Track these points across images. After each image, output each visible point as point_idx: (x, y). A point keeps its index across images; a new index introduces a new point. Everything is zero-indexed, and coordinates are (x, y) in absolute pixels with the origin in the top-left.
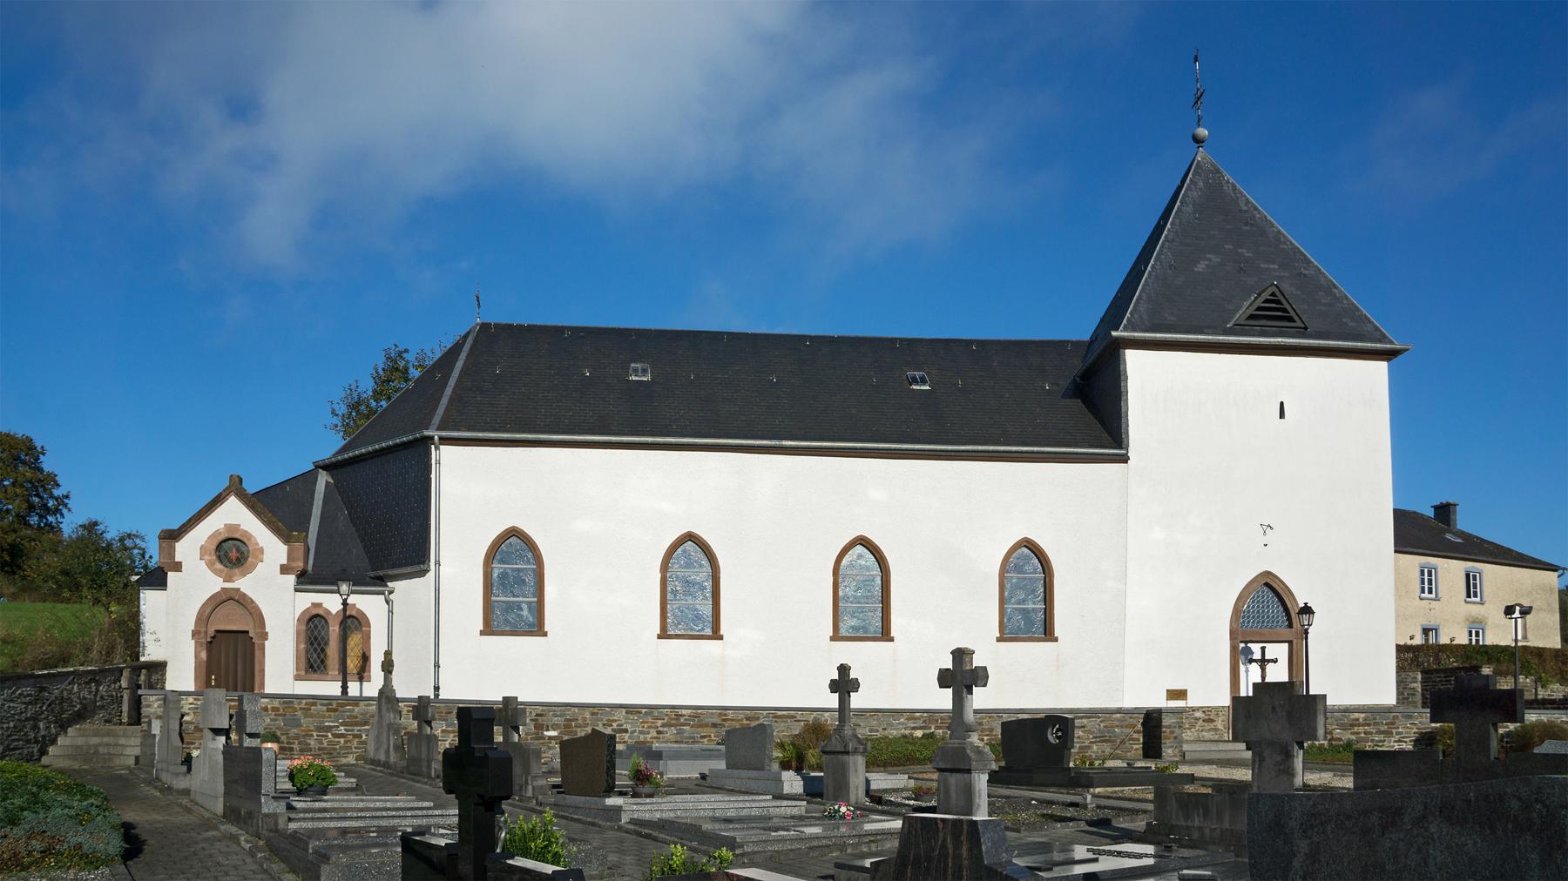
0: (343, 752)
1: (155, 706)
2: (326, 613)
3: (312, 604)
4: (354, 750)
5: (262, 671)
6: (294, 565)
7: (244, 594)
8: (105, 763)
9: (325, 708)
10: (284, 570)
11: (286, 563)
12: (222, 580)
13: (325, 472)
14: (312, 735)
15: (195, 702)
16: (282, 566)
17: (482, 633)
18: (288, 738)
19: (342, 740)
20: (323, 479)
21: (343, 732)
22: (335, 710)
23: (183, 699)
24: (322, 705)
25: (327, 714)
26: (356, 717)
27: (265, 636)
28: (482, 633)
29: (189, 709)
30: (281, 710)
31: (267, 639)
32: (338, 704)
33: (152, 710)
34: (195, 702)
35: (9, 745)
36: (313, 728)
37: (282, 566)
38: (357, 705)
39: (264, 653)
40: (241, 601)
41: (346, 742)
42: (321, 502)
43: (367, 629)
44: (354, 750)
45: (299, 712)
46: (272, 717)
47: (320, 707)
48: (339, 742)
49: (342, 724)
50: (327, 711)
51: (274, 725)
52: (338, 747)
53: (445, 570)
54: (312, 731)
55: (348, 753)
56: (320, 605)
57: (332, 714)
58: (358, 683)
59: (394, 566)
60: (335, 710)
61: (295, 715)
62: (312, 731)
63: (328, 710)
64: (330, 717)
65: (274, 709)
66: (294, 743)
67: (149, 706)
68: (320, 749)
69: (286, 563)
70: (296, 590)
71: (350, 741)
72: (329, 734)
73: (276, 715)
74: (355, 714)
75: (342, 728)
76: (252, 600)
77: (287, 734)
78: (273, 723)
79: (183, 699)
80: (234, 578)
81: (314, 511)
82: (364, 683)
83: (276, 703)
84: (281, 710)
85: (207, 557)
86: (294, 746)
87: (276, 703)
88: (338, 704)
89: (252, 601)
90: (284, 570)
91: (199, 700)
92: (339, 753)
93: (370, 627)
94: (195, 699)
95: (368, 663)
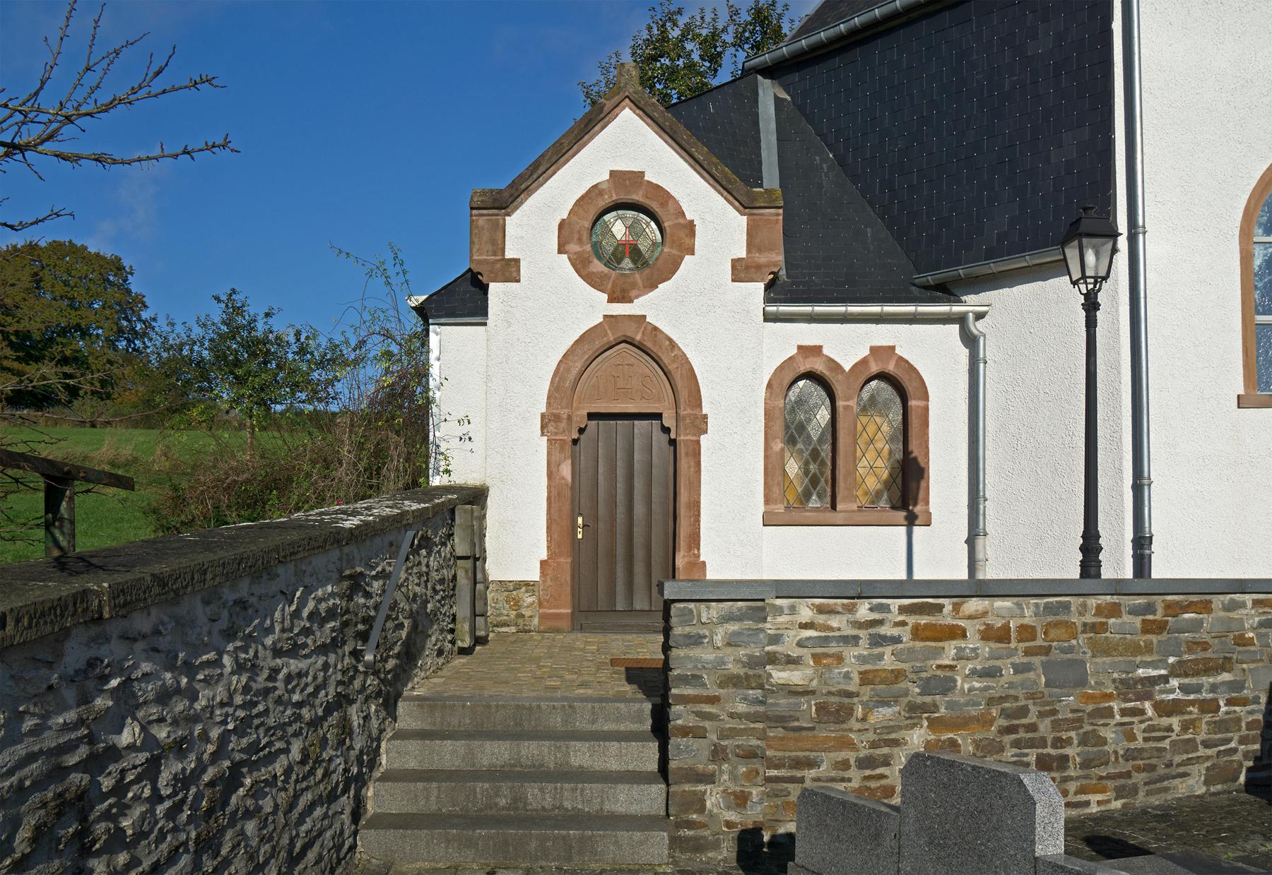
0: (1178, 759)
1: (719, 640)
2: (831, 370)
3: (800, 347)
4: (1202, 752)
5: (695, 506)
6: (762, 259)
7: (655, 329)
8: (569, 859)
9: (1137, 621)
10: (741, 271)
11: (743, 254)
12: (605, 297)
13: (768, 82)
14: (1109, 713)
15: (821, 619)
16: (735, 263)
17: (1241, 402)
18: (1056, 725)
19: (1175, 721)
20: (768, 93)
21: (1178, 695)
22: (1160, 627)
23: (779, 611)
24: (1134, 611)
25: (1142, 639)
26: (1205, 646)
27: (701, 425)
28: (1241, 402)
29: (800, 644)
30: (1041, 635)
31: (705, 432)
32: (1168, 606)
33: (708, 656)
34: (821, 619)
35: (290, 852)
36: (1111, 690)
37: (735, 263)
38: (1206, 607)
39: (698, 464)
40: (649, 344)
41: (1185, 727)
42: (774, 138)
43: (921, 403)
44: (1202, 752)
45: (1082, 638)
46: (1019, 659)
47: (1126, 618)
48: (1169, 729)
49: (1175, 671)
50: (1145, 631)
51: (1022, 685)
52: (1166, 744)
53: (1153, 248)
54: (1109, 697)
55: (1189, 762)
56: (816, 350)
57: (1154, 638)
58: (902, 530)
59: (990, 255)
60: (1160, 627)
61: (1071, 650)
62: (1109, 697)
63: (1148, 628)
64: (1149, 649)
65: (1027, 632)
66: (1069, 742)
67: (696, 640)
68: (1130, 755)
69: (743, 254)
70: (768, 318)
71: (1193, 722)
72: (1147, 705)
73: (1028, 652)
74: (1203, 636)
75: (1174, 682)
76: (671, 340)
77: (1054, 712)
78: (1019, 677)
79: (779, 611)
80: (633, 293)
81: (764, 154)
82: (916, 529)
83: (1029, 612)
84: (1041, 635)
85: (574, 247)
86: (1069, 751)
87: (1029, 612)
88: (1168, 606)
89: (673, 344)
90: (741, 271)
91: (831, 611)
92: (1169, 765)
93: (926, 398)
94: (821, 610)
95: (923, 484)
